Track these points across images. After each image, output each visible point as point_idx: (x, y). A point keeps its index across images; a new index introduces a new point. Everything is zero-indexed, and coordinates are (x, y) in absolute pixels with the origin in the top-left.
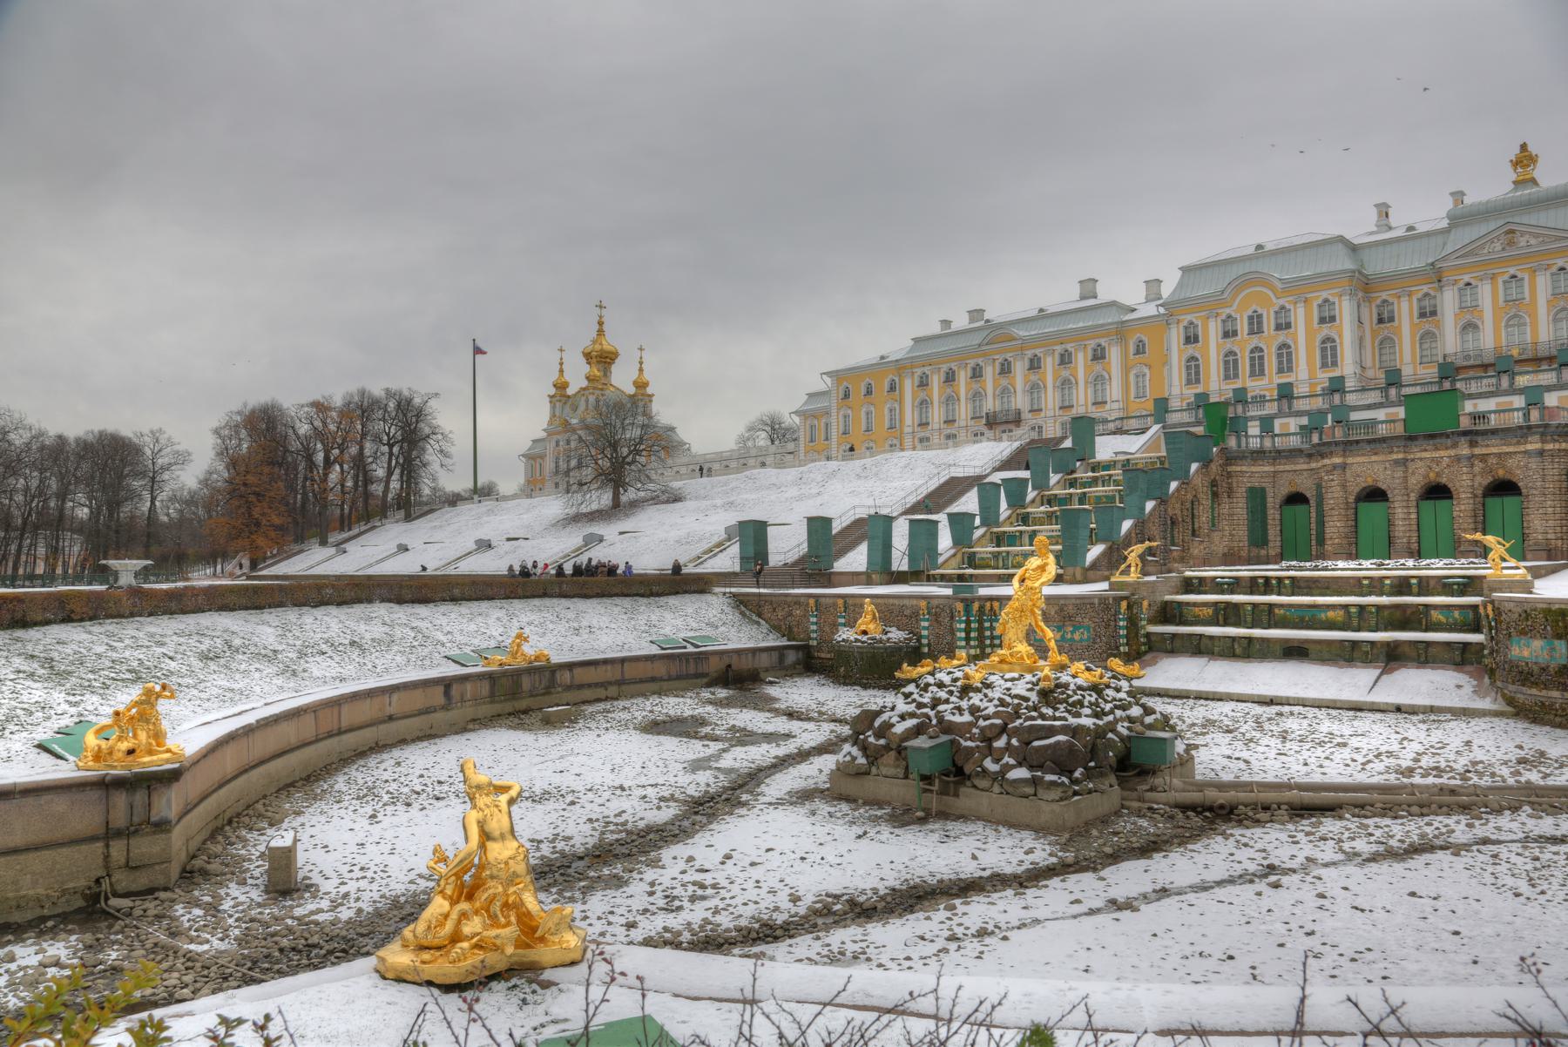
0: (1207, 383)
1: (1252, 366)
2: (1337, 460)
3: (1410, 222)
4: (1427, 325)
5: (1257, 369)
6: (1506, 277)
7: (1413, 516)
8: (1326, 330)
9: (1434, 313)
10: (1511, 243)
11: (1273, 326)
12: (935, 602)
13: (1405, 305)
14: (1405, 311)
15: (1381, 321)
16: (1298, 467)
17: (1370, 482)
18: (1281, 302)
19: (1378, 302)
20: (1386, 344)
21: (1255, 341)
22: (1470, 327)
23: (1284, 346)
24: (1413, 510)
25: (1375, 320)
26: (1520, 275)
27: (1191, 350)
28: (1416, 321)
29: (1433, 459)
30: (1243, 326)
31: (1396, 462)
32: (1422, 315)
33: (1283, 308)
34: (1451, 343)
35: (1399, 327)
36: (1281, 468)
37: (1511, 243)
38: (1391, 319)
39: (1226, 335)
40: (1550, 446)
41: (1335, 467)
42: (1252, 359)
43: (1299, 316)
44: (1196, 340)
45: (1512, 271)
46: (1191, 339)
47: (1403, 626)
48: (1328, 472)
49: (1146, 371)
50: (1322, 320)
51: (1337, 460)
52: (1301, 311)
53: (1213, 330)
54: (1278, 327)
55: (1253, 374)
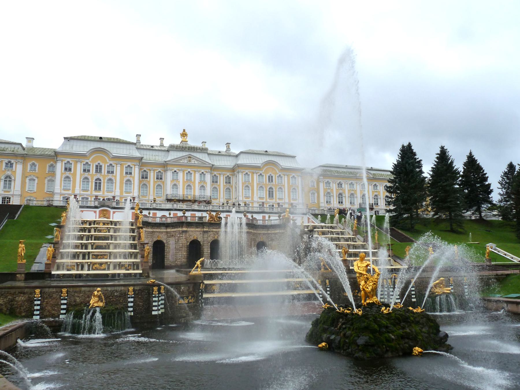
0: (74, 190)
1: (96, 186)
2: (185, 229)
3: (152, 145)
4: (159, 182)
5: (98, 186)
6: (187, 172)
8: (128, 177)
9: (161, 179)
10: (190, 161)
11: (106, 172)
12: (137, 288)
13: (152, 174)
14: (152, 176)
15: (143, 178)
16: (162, 230)
17: (195, 238)
18: (111, 162)
19: (143, 170)
21: (98, 176)
22: (175, 186)
23: (110, 180)
24: (209, 249)
26: (191, 172)
27: (68, 174)
28: (156, 180)
29: (216, 232)
30: (93, 169)
31: (204, 232)
32: (157, 178)
33: (111, 165)
34: (169, 191)
35: (149, 182)
36: (155, 230)
38: (147, 178)
39: (84, 170)
40: (250, 231)
41: (183, 232)
42: (96, 183)
43: (118, 170)
44: (70, 170)
45: (189, 170)
46: (67, 169)
48: (180, 234)
49: (36, 179)
50: (127, 173)
51: (185, 229)
52: (119, 168)
53: (79, 168)
54: (108, 172)
55: (96, 189)
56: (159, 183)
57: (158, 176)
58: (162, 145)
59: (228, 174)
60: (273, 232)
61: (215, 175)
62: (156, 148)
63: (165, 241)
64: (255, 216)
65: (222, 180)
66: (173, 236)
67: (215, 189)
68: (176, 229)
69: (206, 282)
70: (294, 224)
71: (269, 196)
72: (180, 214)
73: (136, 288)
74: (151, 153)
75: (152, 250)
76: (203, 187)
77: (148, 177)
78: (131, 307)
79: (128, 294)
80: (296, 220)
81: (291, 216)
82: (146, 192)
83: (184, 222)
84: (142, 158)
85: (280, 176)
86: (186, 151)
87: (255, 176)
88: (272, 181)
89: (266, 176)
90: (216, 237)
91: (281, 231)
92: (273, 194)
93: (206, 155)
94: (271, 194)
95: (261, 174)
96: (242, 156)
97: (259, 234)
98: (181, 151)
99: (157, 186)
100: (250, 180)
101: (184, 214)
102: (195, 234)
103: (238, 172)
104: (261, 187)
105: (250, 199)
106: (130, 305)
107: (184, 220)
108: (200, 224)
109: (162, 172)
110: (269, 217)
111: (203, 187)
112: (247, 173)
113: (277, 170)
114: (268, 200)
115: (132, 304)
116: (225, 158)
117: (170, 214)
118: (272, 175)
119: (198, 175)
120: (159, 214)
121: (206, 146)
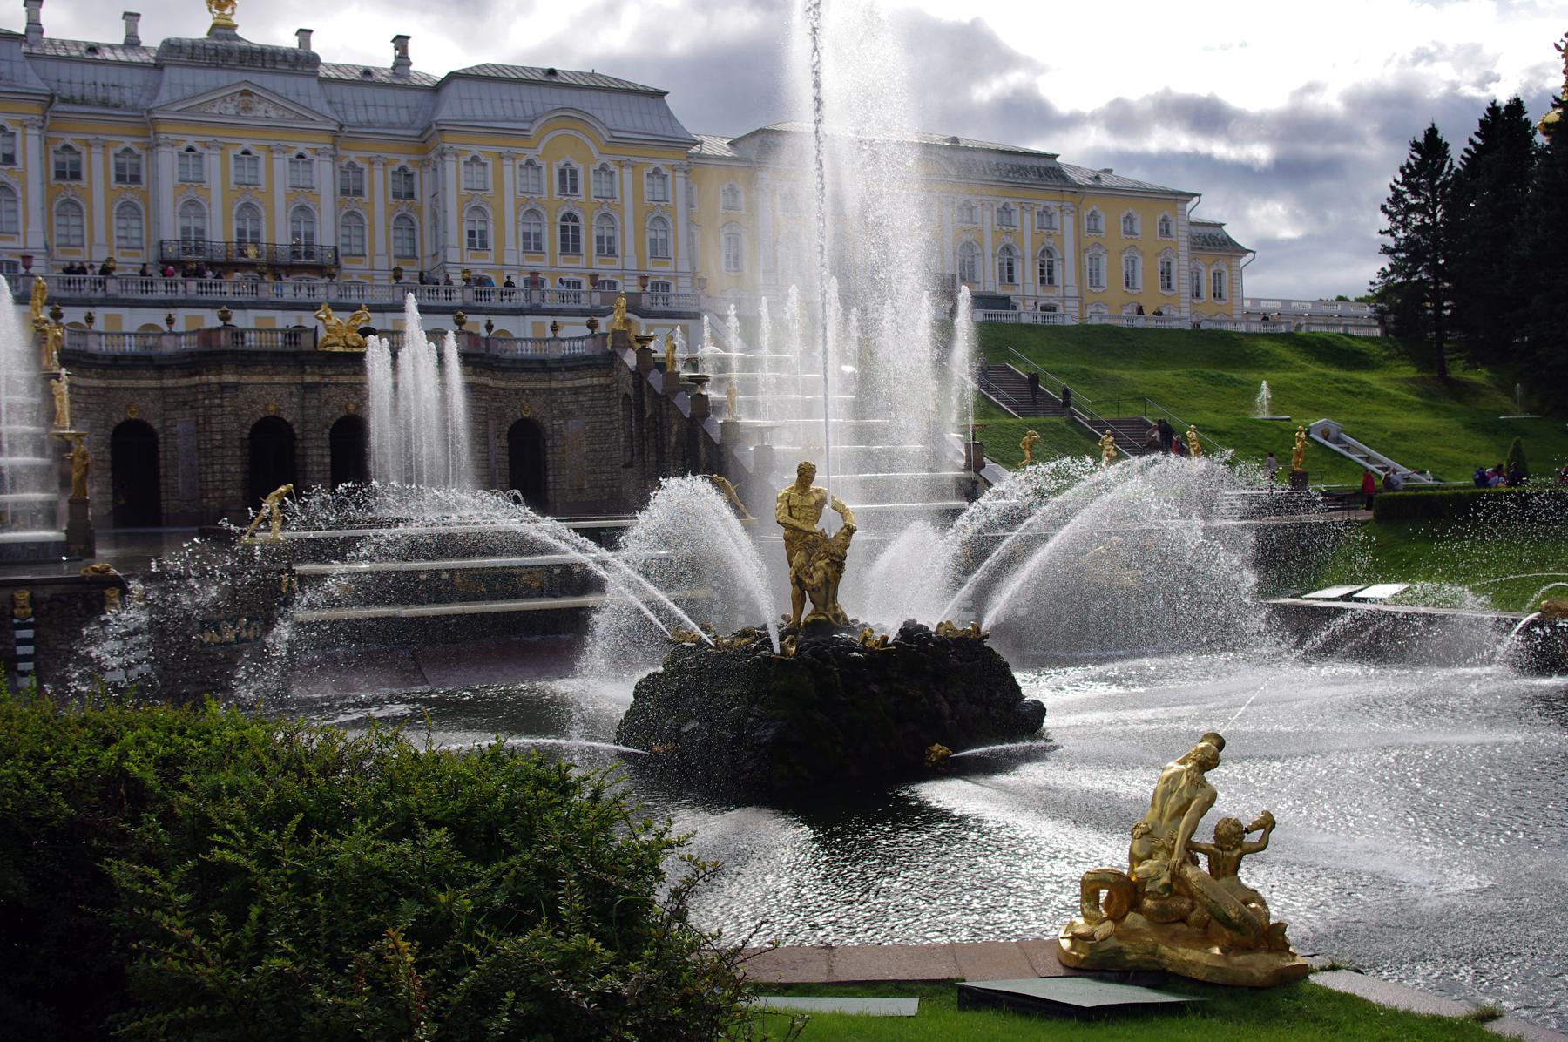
2: (229, 378)
4: (130, 193)
6: (239, 151)
7: (328, 460)
9: (136, 179)
10: (247, 109)
12: (47, 593)
14: (98, 169)
15: (60, 175)
16: (143, 383)
17: (271, 408)
19: (59, 146)
20: (72, 207)
22: (193, 206)
24: (327, 452)
25: (53, 174)
26: (254, 152)
28: (114, 185)
29: (351, 386)
31: (307, 387)
32: (120, 178)
36: (116, 383)
37: (247, 109)
38: (76, 176)
40: (482, 380)
41: (223, 387)
45: (247, 145)
47: (404, 598)
56: (129, 196)
57: (119, 167)
58: (132, 42)
59: (403, 160)
60: (569, 384)
61: (351, 165)
62: (109, 56)
63: (156, 425)
64: (500, 323)
65: (379, 183)
66: (185, 403)
67: (352, 221)
68: (196, 380)
69: (301, 568)
70: (644, 354)
71: (564, 248)
72: (211, 319)
73: (39, 593)
74: (89, 73)
75: (108, 457)
76: (303, 212)
77: (84, 175)
78: (26, 658)
79: (13, 616)
80: (650, 339)
81: (642, 327)
82: (76, 231)
83: (224, 353)
84: (52, 97)
85: (603, 168)
86: (232, 68)
87: (509, 170)
88: (574, 189)
89: (550, 169)
90: (351, 407)
91: (596, 381)
92: (576, 239)
93: (315, 81)
94: (570, 240)
95: (530, 163)
96: (454, 83)
97: (517, 391)
98: (209, 67)
99: (122, 207)
100: (490, 185)
101: (225, 318)
102: (271, 393)
103: (442, 154)
104: (532, 211)
105: (490, 258)
106: (22, 650)
107: (224, 341)
108: (297, 355)
109: (136, 151)
110: (555, 328)
111: (303, 212)
112: (475, 159)
113: (592, 146)
114: (560, 261)
115: (29, 650)
116: (390, 93)
117: (170, 321)
118: (574, 165)
119: (281, 164)
120: (133, 319)
121: (315, 48)
